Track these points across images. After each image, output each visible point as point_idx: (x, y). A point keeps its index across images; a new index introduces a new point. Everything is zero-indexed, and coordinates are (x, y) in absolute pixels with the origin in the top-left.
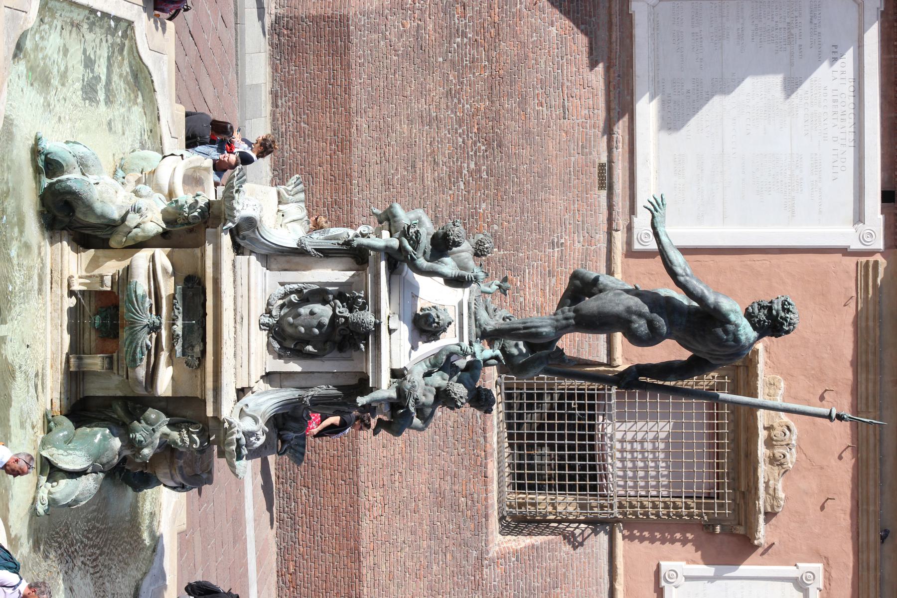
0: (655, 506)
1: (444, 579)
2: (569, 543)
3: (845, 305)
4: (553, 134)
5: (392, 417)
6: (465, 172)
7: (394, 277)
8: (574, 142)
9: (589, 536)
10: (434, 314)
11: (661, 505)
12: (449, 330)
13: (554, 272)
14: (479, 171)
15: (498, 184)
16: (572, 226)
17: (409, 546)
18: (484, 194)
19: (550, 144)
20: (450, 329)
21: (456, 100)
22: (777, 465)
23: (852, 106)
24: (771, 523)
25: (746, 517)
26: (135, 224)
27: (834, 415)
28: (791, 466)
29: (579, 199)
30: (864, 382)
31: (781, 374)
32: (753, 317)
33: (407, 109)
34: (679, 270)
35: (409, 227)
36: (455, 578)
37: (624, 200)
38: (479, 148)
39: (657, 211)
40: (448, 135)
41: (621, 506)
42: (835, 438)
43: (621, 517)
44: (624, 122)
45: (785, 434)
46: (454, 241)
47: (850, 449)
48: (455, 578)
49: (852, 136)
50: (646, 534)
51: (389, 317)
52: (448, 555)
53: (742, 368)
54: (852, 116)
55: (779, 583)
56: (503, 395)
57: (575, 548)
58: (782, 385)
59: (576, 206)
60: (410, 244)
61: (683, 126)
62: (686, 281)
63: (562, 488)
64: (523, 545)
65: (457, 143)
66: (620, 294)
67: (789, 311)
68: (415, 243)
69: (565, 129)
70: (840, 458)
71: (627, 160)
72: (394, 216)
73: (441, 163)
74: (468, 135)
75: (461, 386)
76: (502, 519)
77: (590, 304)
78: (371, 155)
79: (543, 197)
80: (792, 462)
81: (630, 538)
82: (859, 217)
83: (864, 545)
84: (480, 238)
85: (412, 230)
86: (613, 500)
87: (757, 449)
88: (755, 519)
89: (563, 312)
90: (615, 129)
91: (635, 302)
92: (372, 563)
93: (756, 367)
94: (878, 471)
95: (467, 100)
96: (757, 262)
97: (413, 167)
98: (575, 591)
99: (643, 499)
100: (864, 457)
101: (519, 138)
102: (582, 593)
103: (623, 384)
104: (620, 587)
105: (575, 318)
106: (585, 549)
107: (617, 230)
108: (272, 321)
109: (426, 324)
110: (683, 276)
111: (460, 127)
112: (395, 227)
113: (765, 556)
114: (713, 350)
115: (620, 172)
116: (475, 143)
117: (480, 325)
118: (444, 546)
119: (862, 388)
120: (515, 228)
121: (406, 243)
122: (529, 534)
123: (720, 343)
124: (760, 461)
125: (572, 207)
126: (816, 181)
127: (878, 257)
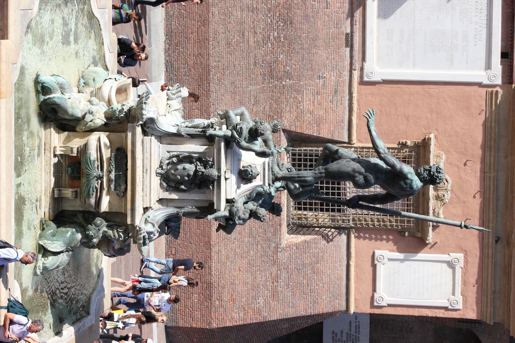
0: (372, 221)
1: (257, 259)
2: (325, 239)
3: (479, 114)
4: (321, 17)
5: (226, 223)
6: (272, 38)
7: (229, 151)
8: (332, 21)
9: (336, 236)
10: (249, 170)
11: (376, 220)
12: (257, 177)
13: (319, 92)
14: (280, 37)
15: (290, 44)
16: (330, 67)
17: (238, 241)
18: (282, 50)
19: (319, 22)
20: (258, 177)
22: (440, 200)
23: (486, 5)
24: (435, 231)
25: (422, 229)
26: (90, 121)
27: (463, 225)
28: (447, 201)
29: (334, 52)
30: (488, 156)
31: (443, 151)
32: (421, 175)
33: (240, 3)
34: (381, 151)
35: (237, 125)
36: (263, 258)
37: (359, 53)
38: (280, 24)
39: (370, 118)
40: (263, 18)
41: (354, 220)
42: (472, 186)
43: (353, 226)
44: (360, 10)
45: (445, 184)
46: (261, 133)
47: (479, 193)
48: (263, 258)
49: (485, 22)
50: (367, 235)
51: (225, 172)
52: (259, 246)
53: (422, 147)
54: (486, 11)
55: (439, 264)
56: (291, 159)
57: (328, 242)
58: (444, 157)
59: (333, 56)
60: (237, 134)
61: (392, 14)
62: (385, 156)
63: (322, 210)
64: (300, 240)
65: (267, 22)
66: (349, 161)
67: (440, 172)
68: (240, 134)
69: (328, 14)
70: (474, 197)
71: (361, 32)
72: (229, 117)
73: (258, 33)
74: (273, 18)
75: (264, 209)
76: (288, 225)
77: (334, 166)
78: (220, 29)
79: (315, 52)
80: (448, 199)
81: (358, 237)
82: (488, 66)
83: (486, 245)
84: (275, 123)
85: (238, 127)
86: (349, 216)
87: (429, 192)
88: (427, 229)
89: (319, 170)
90: (355, 14)
91: (357, 166)
92: (217, 250)
93: (429, 147)
94: (495, 205)
96: (432, 89)
97: (243, 35)
98: (328, 265)
99: (366, 216)
100: (488, 197)
101: (302, 19)
102: (332, 266)
103: (350, 206)
104: (352, 263)
105: (325, 173)
106: (334, 243)
107: (355, 70)
108: (163, 172)
109: (245, 175)
110: (383, 154)
111: (269, 13)
112: (229, 123)
113: (432, 249)
114: (399, 192)
115: (357, 38)
116: (277, 22)
117: (274, 174)
118: (257, 241)
119: (487, 160)
120: (299, 68)
121: (235, 133)
122: (303, 234)
123: (402, 189)
124: (430, 198)
125: (330, 57)
126: (465, 46)
127: (498, 89)
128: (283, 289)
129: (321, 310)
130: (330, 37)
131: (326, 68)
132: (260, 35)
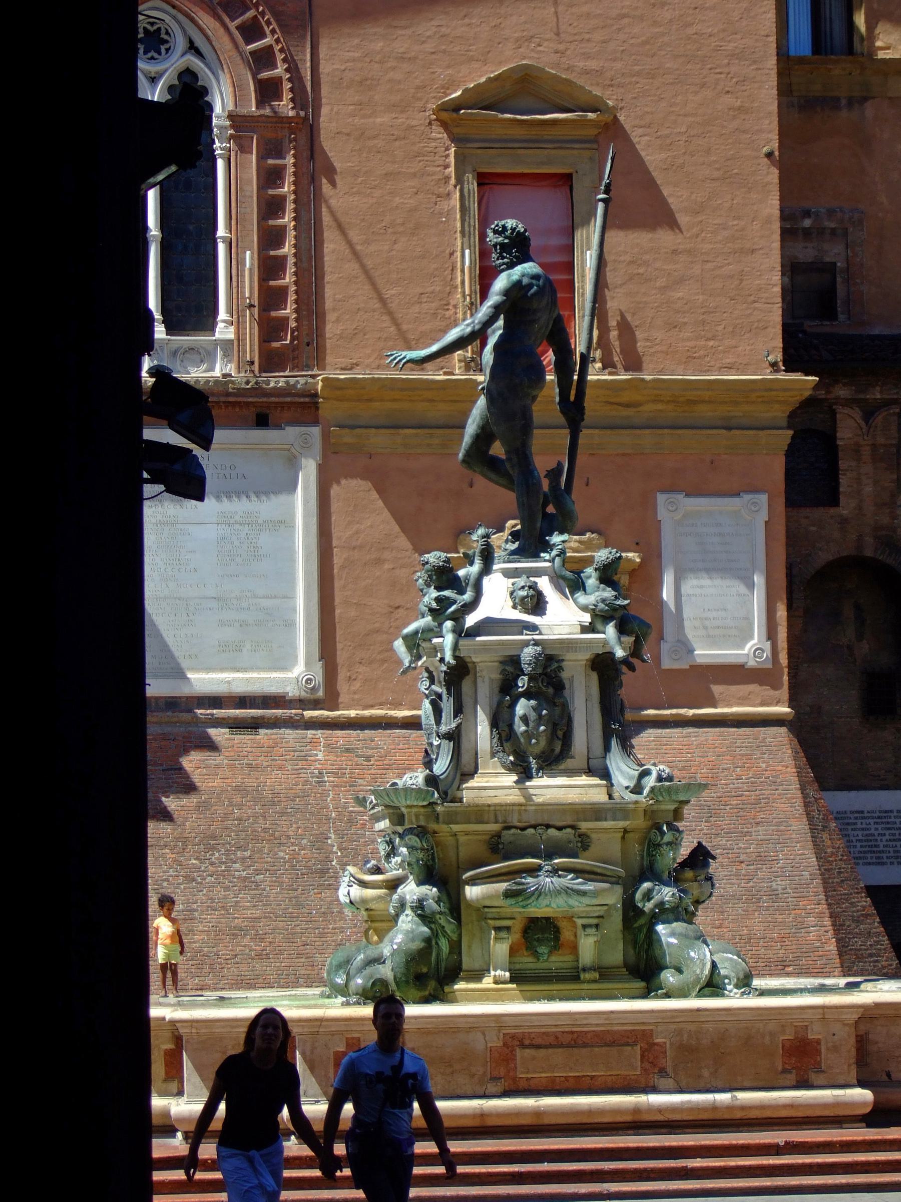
8: (207, 760)
14: (243, 859)
15: (256, 839)
21: (165, 884)
38: (218, 859)
39: (404, 358)
40: (204, 892)
62: (479, 323)
74: (204, 871)
78: (230, 974)
95: (164, 872)
98: (697, 759)
101: (205, 818)
110: (474, 327)
116: (212, 864)
120: (304, 822)
123: (541, 291)
128: (752, 844)
129: (789, 769)
130: (239, 764)
131: (302, 769)
132: (241, 896)
